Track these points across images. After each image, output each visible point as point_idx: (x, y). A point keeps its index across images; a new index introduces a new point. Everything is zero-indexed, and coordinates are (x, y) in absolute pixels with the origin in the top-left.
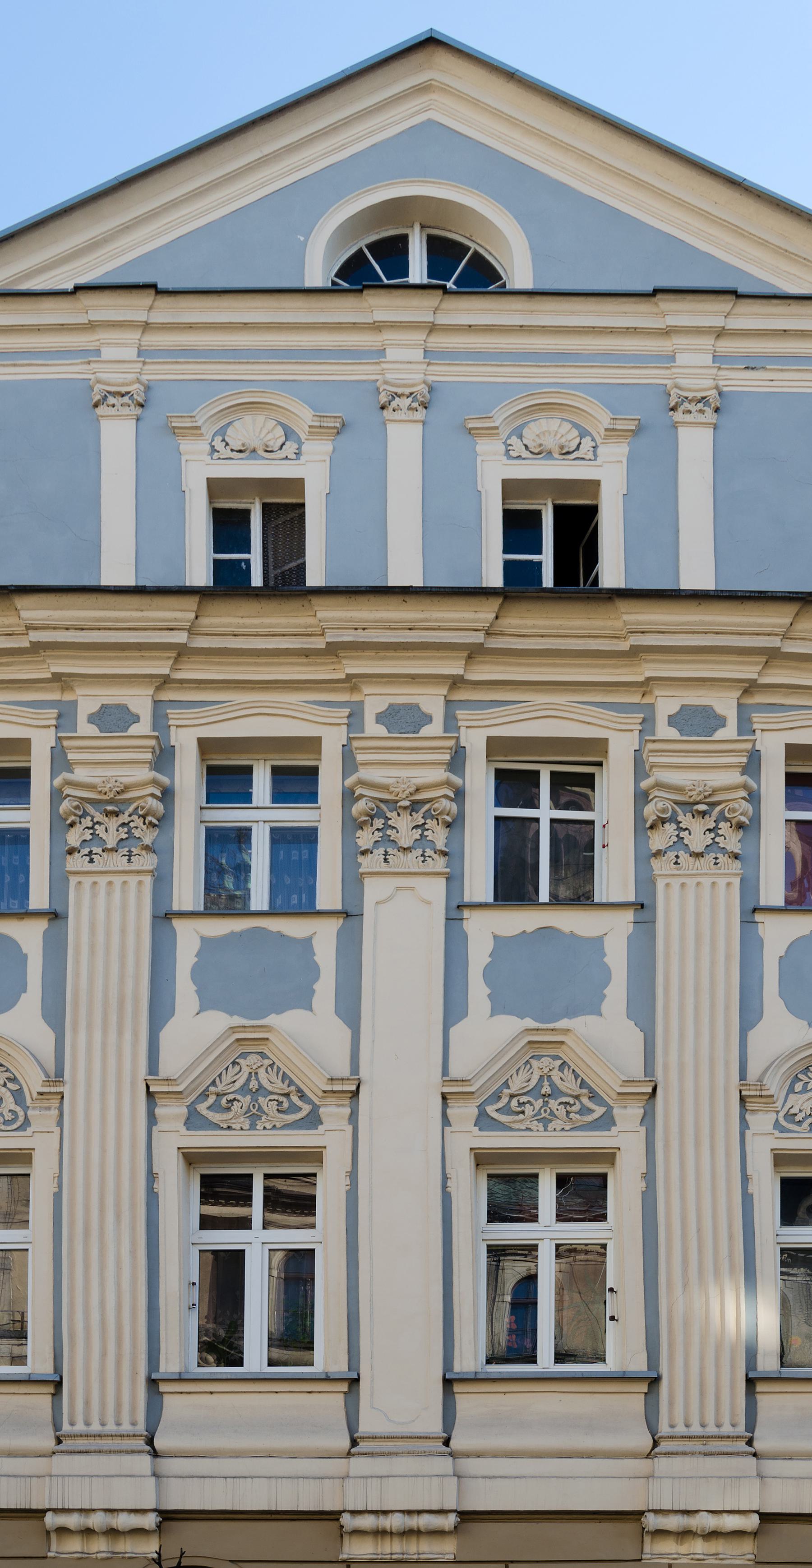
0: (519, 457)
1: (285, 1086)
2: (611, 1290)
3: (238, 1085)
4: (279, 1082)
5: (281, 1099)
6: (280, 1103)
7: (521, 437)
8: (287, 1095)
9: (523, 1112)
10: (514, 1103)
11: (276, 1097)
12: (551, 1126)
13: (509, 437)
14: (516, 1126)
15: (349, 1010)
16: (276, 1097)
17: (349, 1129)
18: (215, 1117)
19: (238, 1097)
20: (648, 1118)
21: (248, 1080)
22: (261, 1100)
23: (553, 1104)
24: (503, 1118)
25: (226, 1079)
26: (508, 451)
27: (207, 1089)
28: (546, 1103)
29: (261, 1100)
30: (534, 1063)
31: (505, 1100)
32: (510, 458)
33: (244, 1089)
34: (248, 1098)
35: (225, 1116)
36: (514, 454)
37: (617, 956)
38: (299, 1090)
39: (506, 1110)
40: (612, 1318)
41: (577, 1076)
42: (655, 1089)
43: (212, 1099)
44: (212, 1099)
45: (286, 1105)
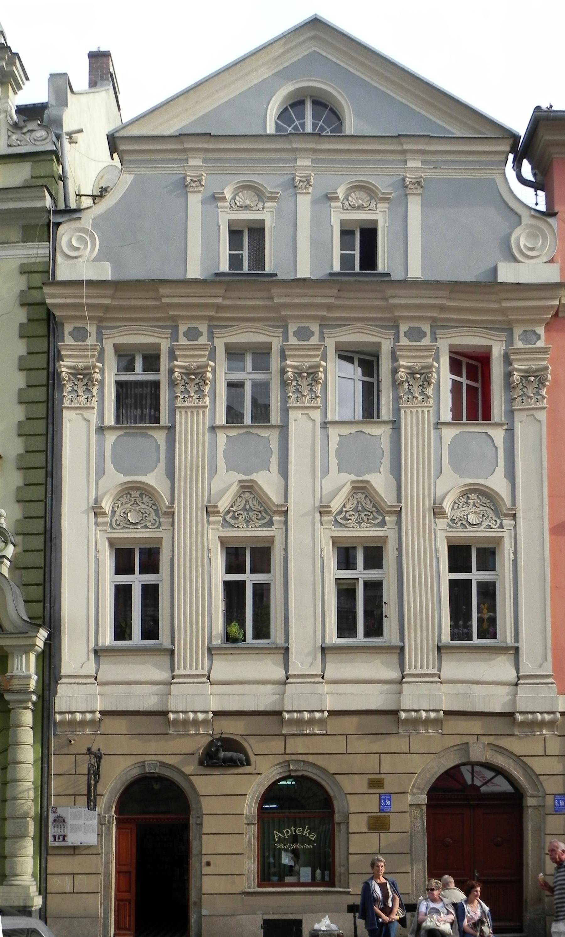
0: (347, 209)
1: (259, 508)
2: (385, 603)
3: (241, 507)
4: (257, 505)
5: (258, 513)
6: (258, 515)
7: (348, 200)
8: (260, 512)
9: (351, 519)
10: (347, 515)
11: (256, 512)
12: (362, 525)
13: (343, 200)
14: (348, 526)
15: (284, 472)
16: (256, 512)
17: (284, 527)
18: (232, 522)
19: (242, 513)
20: (399, 523)
21: (245, 504)
22: (250, 513)
23: (362, 515)
24: (344, 522)
25: (237, 504)
26: (343, 206)
27: (229, 509)
28: (360, 515)
29: (250, 513)
30: (355, 495)
31: (344, 513)
32: (344, 209)
33: (244, 509)
34: (245, 513)
35: (236, 521)
36: (345, 208)
37: (385, 444)
38: (265, 509)
39: (345, 518)
40: (386, 616)
41: (371, 502)
42: (401, 509)
43: (231, 514)
44: (231, 514)
45: (260, 516)
